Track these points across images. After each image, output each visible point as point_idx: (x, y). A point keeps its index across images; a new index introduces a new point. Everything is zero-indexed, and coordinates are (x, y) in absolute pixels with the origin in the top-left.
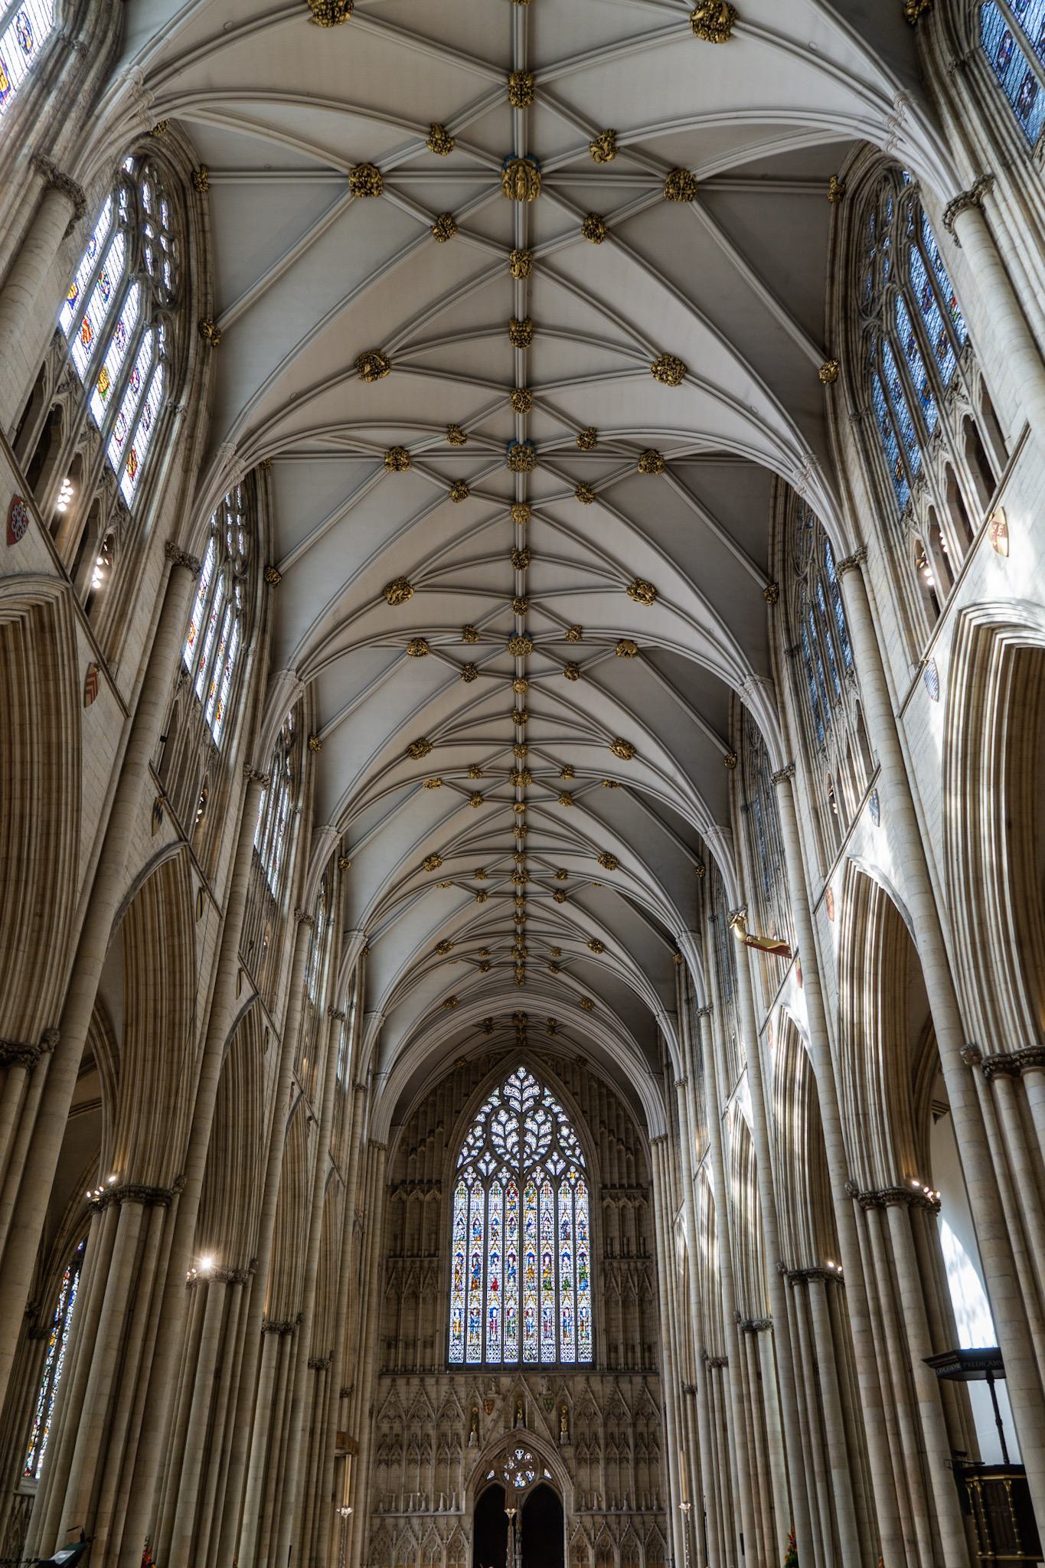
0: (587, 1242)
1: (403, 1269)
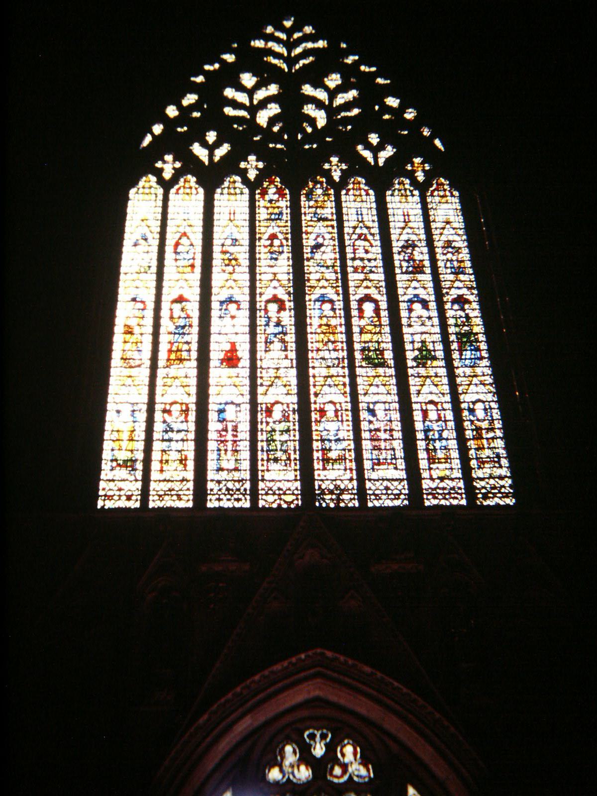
0: (468, 278)
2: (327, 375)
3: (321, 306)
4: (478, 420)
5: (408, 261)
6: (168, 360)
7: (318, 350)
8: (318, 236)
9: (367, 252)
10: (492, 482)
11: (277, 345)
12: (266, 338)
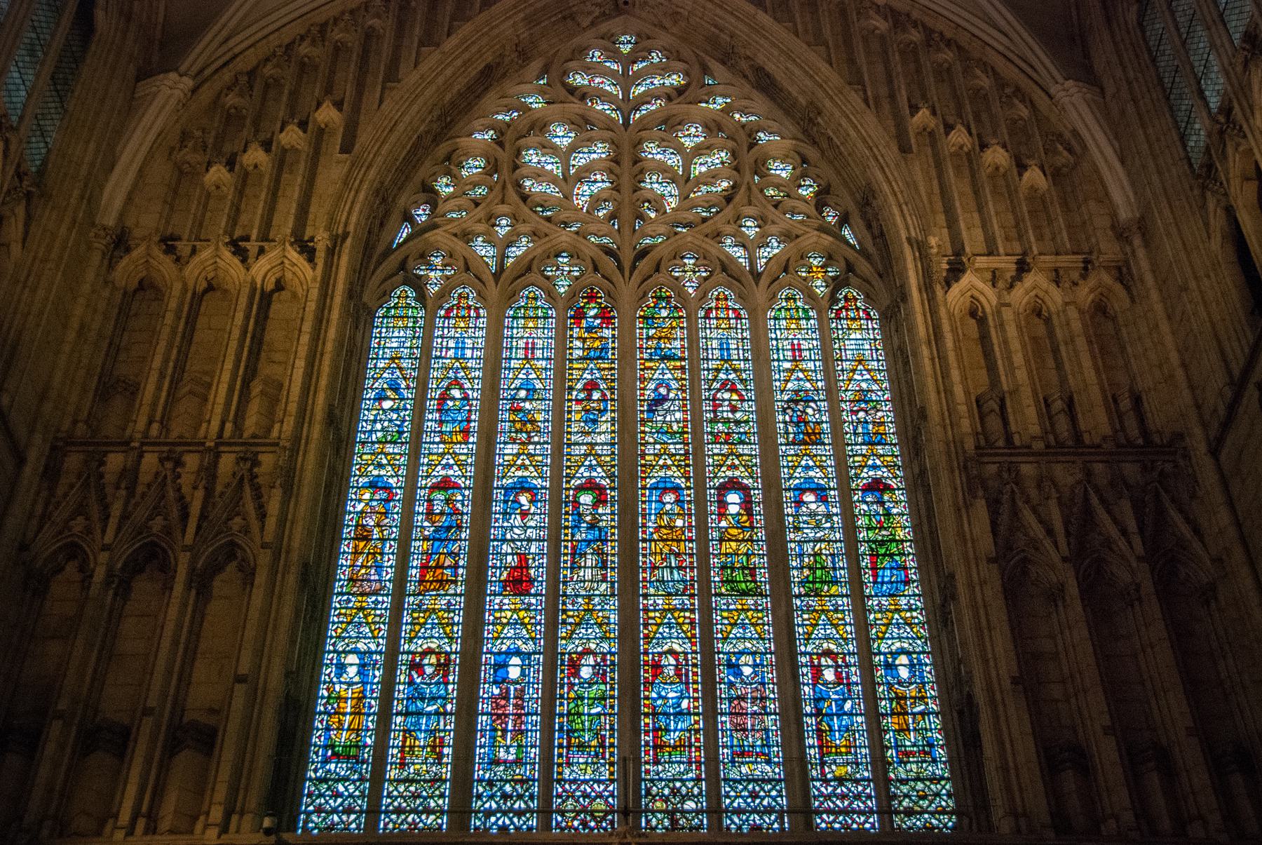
0: (890, 451)
1: (130, 475)
2: (667, 607)
3: (660, 496)
4: (899, 683)
5: (797, 424)
6: (421, 581)
7: (654, 568)
8: (659, 385)
9: (734, 410)
10: (920, 786)
11: (590, 560)
12: (573, 547)
